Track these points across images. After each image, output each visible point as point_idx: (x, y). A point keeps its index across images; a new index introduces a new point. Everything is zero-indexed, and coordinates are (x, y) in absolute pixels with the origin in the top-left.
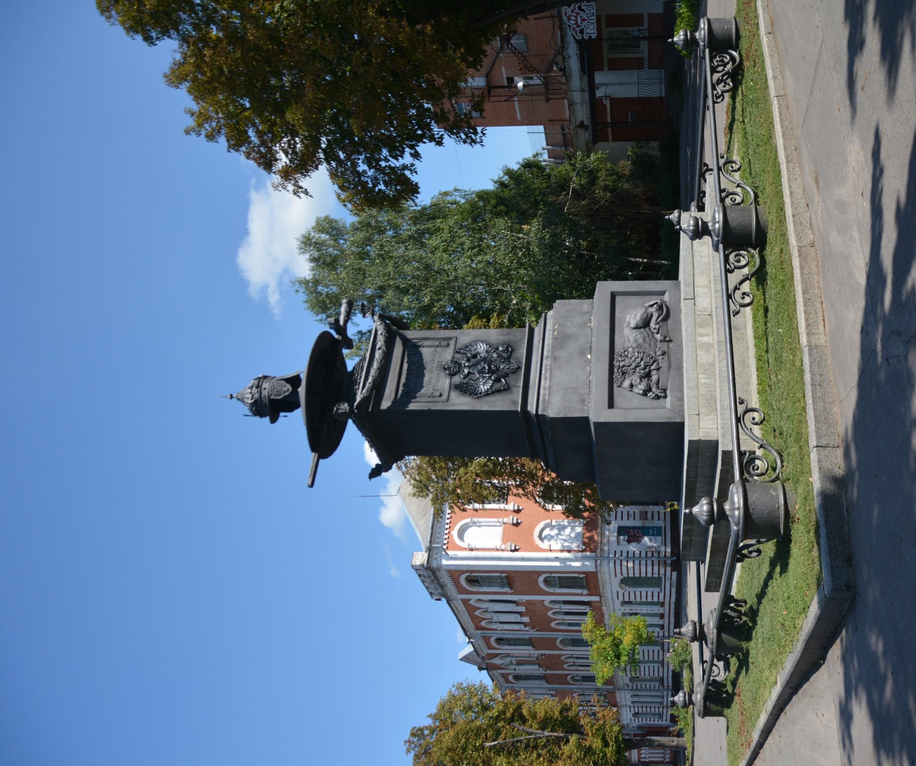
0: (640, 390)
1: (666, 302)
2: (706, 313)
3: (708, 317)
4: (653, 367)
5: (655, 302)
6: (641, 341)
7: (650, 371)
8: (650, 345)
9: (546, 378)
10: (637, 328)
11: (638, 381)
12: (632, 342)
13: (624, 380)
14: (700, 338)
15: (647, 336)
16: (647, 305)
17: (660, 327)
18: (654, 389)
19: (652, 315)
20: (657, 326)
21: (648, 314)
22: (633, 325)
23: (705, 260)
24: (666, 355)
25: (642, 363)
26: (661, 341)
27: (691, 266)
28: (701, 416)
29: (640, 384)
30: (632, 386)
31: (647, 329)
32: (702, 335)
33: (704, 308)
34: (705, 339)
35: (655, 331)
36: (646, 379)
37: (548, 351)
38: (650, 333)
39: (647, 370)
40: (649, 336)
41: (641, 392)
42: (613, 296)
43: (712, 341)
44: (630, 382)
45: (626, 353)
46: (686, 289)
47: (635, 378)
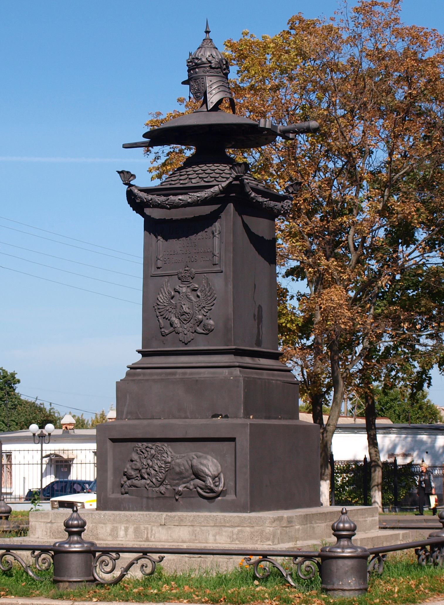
0: (127, 469)
1: (225, 496)
2: (149, 536)
3: (145, 536)
4: (148, 482)
5: (222, 485)
6: (177, 469)
7: (144, 479)
8: (174, 480)
9: (161, 374)
10: (192, 467)
11: (134, 467)
12: (177, 461)
13: (137, 453)
14: (123, 528)
15: (184, 476)
16: (222, 476)
17: (191, 490)
18: (129, 482)
19: (204, 481)
20: (191, 487)
21: (203, 477)
22: (195, 462)
23: (211, 538)
24: (161, 495)
25: (153, 472)
26: (174, 490)
27: (203, 524)
28: (49, 525)
29: (132, 468)
30: (132, 461)
31: (193, 477)
32: (126, 529)
33: (154, 534)
34: (122, 533)
35: (188, 485)
36: (139, 475)
37: (191, 374)
38: (189, 479)
39: (146, 476)
40: (184, 478)
41: (126, 470)
42: (233, 440)
43: (120, 539)
44: (133, 459)
45: (165, 455)
46: (177, 518)
47: (139, 465)
